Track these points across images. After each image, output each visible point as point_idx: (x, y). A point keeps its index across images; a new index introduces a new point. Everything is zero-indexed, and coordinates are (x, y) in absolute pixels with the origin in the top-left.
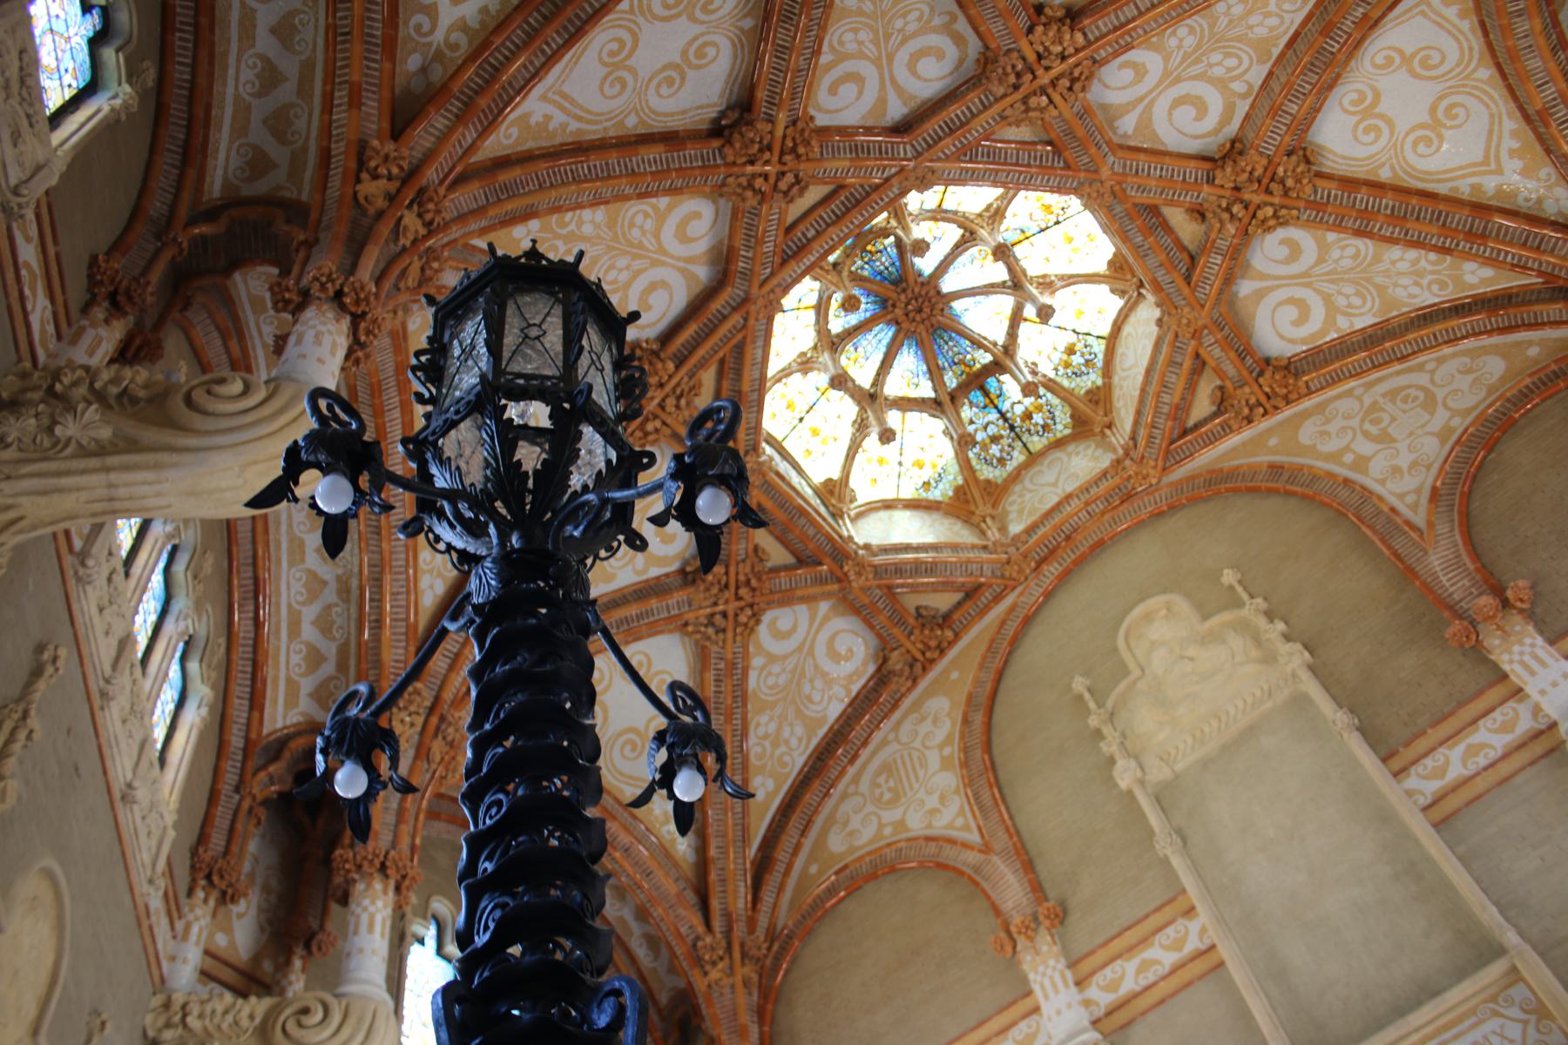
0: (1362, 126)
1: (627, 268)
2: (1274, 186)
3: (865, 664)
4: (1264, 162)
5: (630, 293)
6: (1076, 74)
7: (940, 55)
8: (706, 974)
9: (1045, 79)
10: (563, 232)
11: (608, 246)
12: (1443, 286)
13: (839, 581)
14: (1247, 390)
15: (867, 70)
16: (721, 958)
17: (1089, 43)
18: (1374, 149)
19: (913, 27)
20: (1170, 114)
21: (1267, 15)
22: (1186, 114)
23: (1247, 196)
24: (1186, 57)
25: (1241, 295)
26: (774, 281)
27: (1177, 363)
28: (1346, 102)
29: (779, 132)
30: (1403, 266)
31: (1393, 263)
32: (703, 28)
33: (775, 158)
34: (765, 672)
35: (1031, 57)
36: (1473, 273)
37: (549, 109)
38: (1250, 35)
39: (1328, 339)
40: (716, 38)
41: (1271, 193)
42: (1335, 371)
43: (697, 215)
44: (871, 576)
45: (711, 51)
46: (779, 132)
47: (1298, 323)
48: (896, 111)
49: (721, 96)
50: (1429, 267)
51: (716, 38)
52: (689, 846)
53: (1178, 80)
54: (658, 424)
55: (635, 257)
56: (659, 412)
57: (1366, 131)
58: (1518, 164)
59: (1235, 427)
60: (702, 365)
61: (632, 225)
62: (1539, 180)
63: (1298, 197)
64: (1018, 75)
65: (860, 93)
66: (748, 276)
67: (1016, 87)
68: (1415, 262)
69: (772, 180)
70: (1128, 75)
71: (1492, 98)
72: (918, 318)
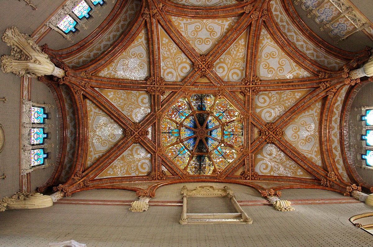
0: (294, 135)
1: (171, 65)
2: (275, 133)
3: (146, 173)
4: (276, 127)
5: (168, 69)
6: (256, 88)
7: (238, 76)
8: (75, 176)
9: (251, 86)
10: (169, 47)
11: (172, 58)
12: (293, 173)
13: (156, 150)
14: (249, 172)
15: (226, 69)
16: (80, 177)
17: (261, 84)
18: (294, 140)
19: (237, 66)
20: (265, 113)
21: (289, 102)
22: (268, 115)
23: (269, 131)
24: (273, 103)
25: (258, 158)
26: (189, 87)
27: (239, 159)
28: (294, 128)
29: (209, 60)
30: (288, 166)
31: (287, 164)
32: (210, 37)
33: (205, 64)
34: (128, 155)
35: (251, 80)
36: (299, 172)
37: (183, 27)
38: (285, 105)
39: (268, 175)
40: (211, 41)
41: (274, 133)
42: (266, 178)
43: (186, 68)
44: (161, 154)
45: (208, 43)
46: (209, 60)
47: (264, 169)
48: (226, 79)
49: (204, 52)
50: (292, 168)
51: (211, 41)
52: (90, 164)
53: (269, 107)
54: (154, 89)
55: (173, 64)
56: (156, 88)
57: (295, 136)
58: (315, 154)
59: (242, 179)
60: (168, 88)
61: (177, 59)
62: (317, 158)
63: (278, 137)
64: (247, 82)
65: (223, 72)
66: (185, 82)
67: (246, 85)
68: (290, 166)
69: (202, 68)
70: (262, 101)
71: (316, 139)
72: (200, 134)
